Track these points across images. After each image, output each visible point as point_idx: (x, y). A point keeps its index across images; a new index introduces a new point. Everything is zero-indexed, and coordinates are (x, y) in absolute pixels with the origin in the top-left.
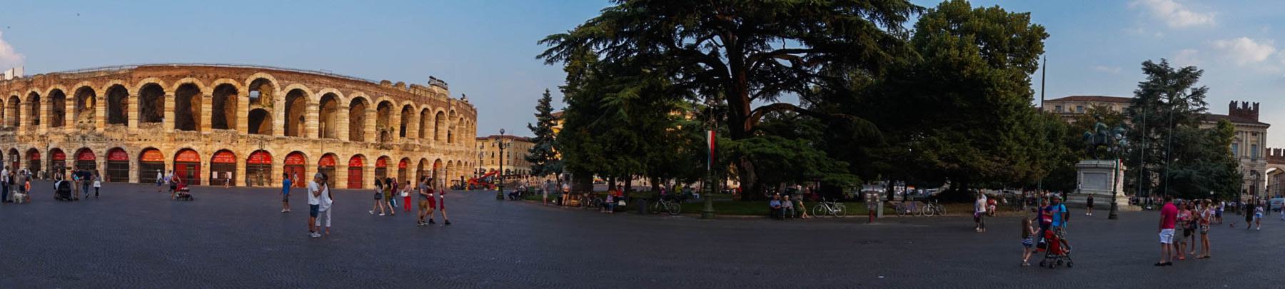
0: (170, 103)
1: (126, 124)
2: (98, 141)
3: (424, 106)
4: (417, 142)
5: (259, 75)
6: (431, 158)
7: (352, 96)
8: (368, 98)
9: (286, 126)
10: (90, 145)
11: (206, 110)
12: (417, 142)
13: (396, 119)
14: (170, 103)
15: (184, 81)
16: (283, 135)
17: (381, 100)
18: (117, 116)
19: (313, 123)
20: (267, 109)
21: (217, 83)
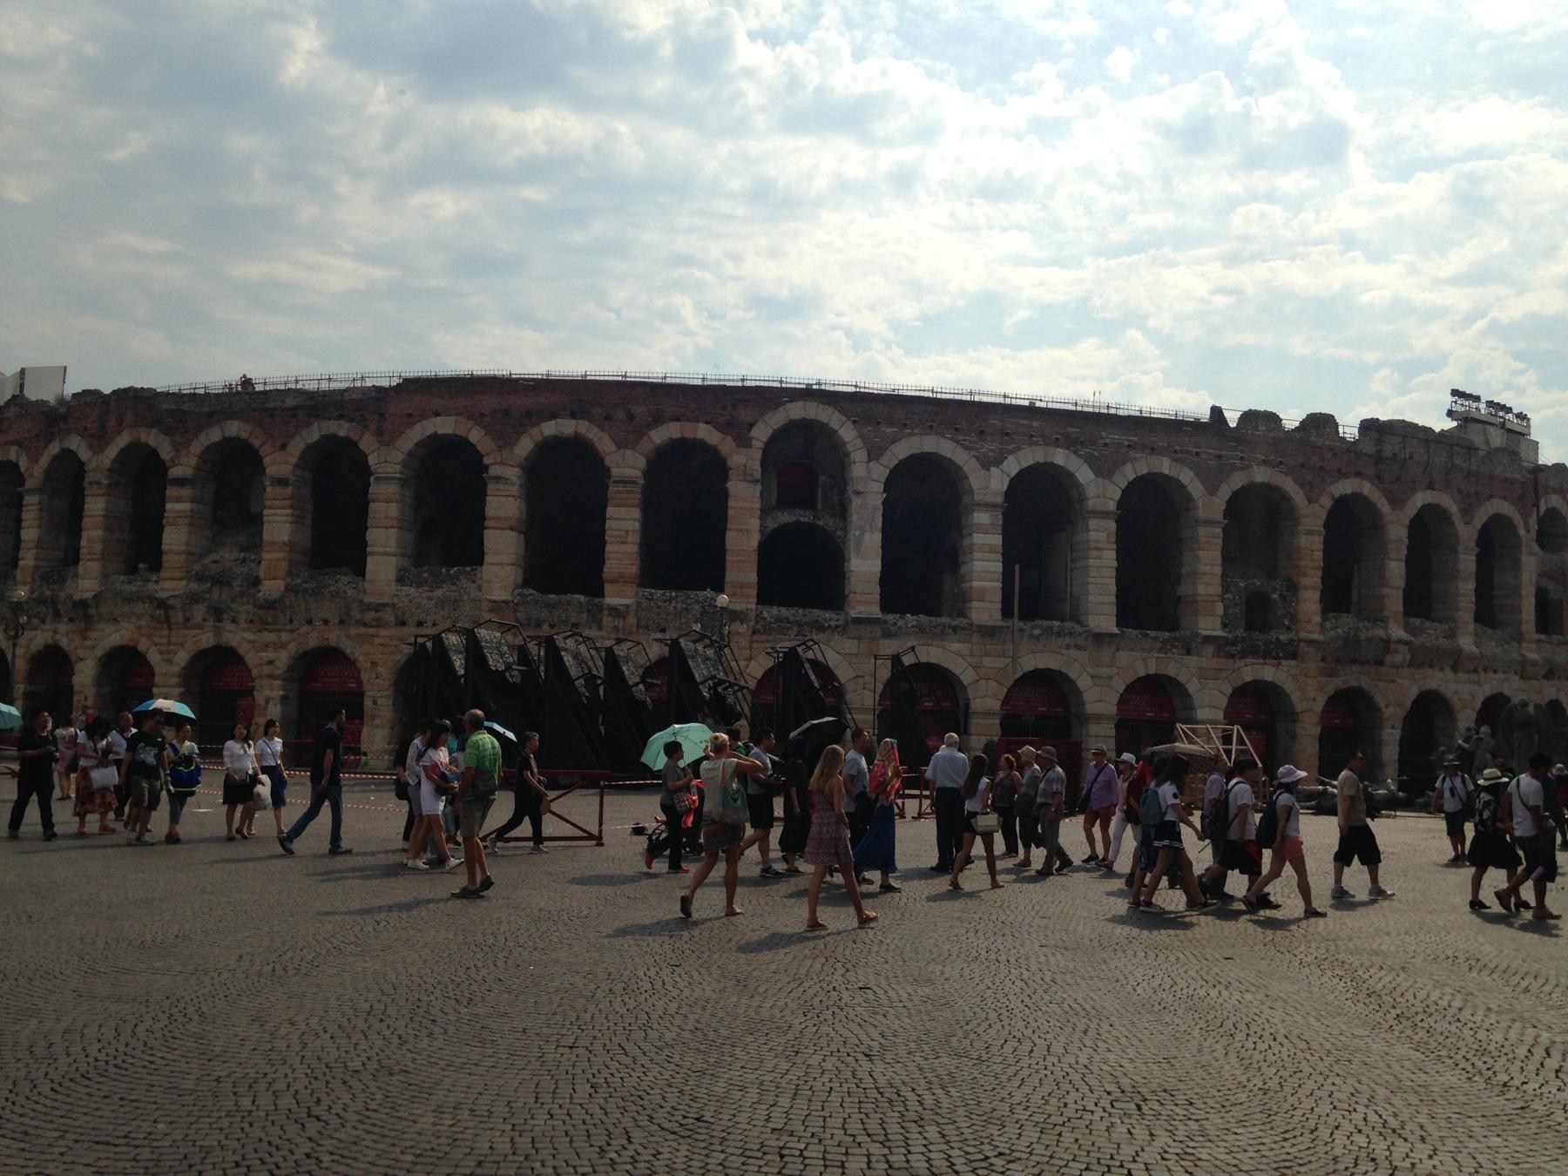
0: (504, 504)
1: (359, 570)
2: (261, 625)
3: (1421, 499)
4: (1397, 632)
5: (796, 411)
6: (1466, 694)
7: (1129, 473)
8: (1186, 476)
9: (884, 581)
10: (238, 637)
11: (623, 525)
12: (1397, 632)
13: (1310, 545)
14: (504, 504)
15: (549, 428)
16: (874, 611)
17: (1237, 481)
18: (336, 543)
19: (984, 564)
20: (827, 522)
21: (661, 435)
